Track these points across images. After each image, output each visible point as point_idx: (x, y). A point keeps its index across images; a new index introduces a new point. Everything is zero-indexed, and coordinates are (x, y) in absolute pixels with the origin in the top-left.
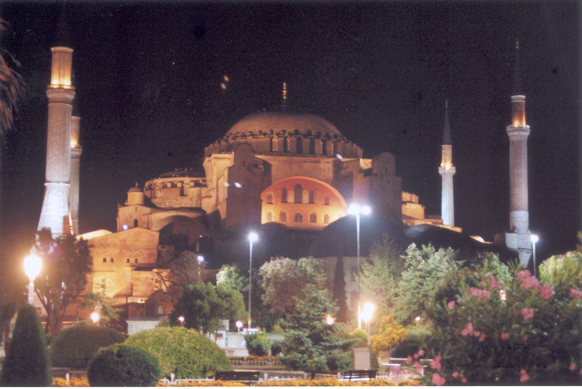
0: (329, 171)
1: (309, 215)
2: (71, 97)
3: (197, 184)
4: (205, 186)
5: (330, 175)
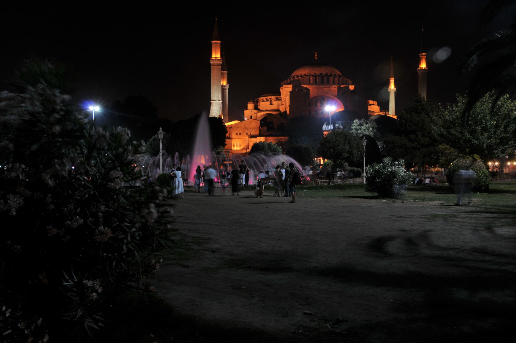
0: (335, 91)
2: (221, 63)
3: (277, 99)
4: (281, 100)
5: (336, 93)
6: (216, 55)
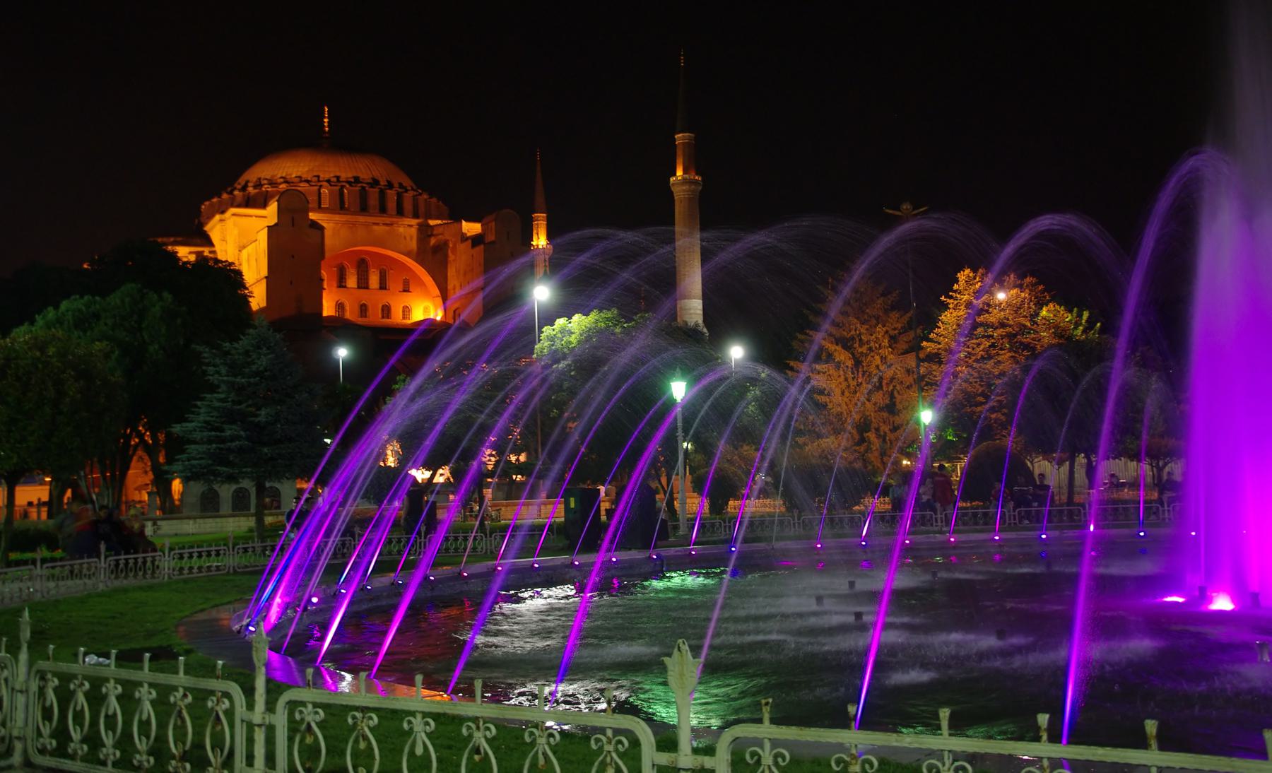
1: (380, 306)
5: (413, 245)
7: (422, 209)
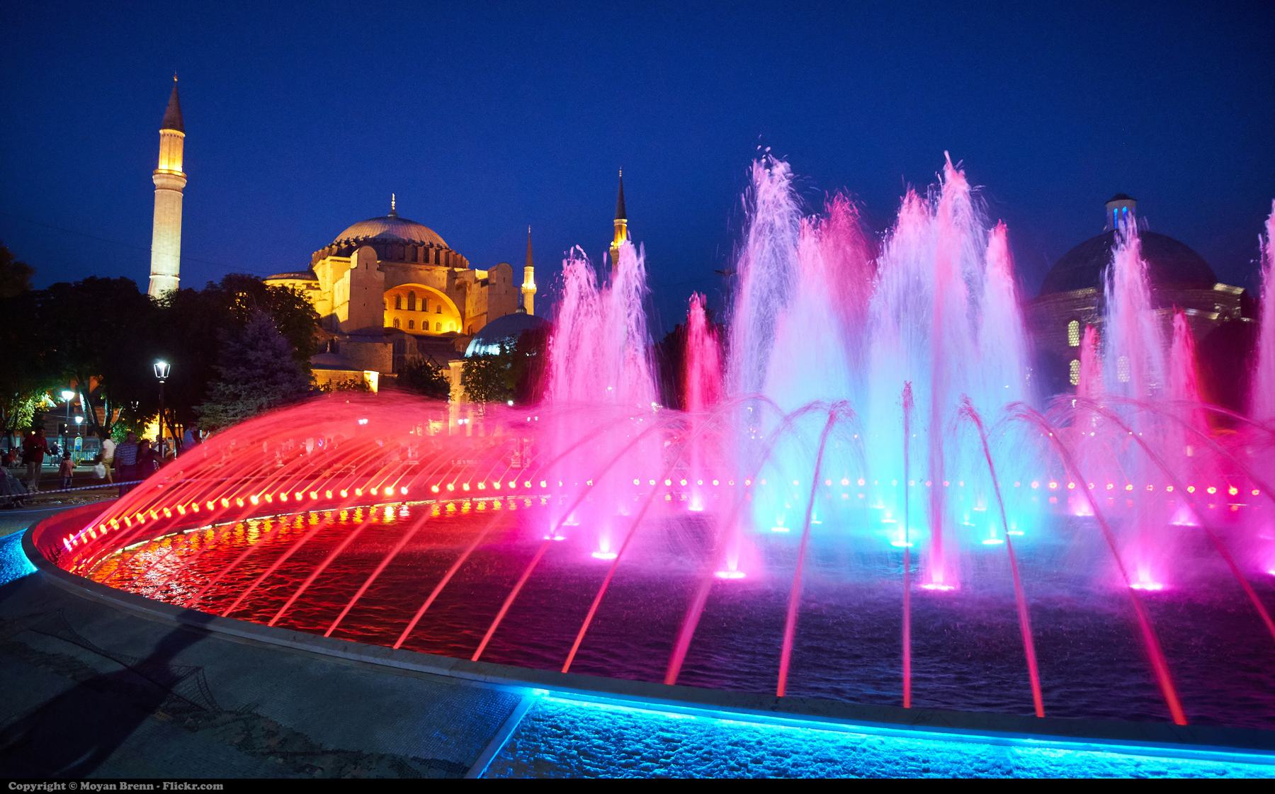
0: (443, 279)
2: (182, 184)
4: (319, 289)
5: (444, 284)
6: (170, 164)
7: (451, 262)
